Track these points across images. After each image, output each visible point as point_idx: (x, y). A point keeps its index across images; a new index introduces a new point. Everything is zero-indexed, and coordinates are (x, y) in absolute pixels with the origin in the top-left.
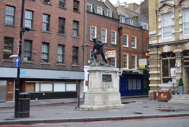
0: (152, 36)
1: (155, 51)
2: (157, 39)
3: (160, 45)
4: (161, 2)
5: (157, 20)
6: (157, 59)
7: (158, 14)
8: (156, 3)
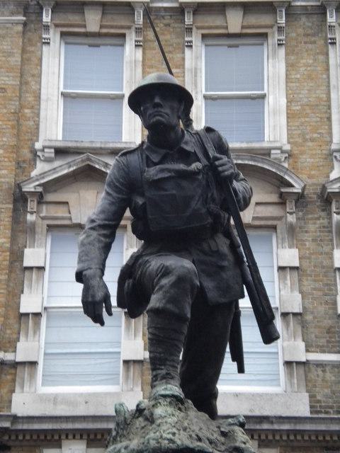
3: (24, 432)
4: (60, 152)
5: (17, 256)
7: (30, 218)
8: (16, 149)
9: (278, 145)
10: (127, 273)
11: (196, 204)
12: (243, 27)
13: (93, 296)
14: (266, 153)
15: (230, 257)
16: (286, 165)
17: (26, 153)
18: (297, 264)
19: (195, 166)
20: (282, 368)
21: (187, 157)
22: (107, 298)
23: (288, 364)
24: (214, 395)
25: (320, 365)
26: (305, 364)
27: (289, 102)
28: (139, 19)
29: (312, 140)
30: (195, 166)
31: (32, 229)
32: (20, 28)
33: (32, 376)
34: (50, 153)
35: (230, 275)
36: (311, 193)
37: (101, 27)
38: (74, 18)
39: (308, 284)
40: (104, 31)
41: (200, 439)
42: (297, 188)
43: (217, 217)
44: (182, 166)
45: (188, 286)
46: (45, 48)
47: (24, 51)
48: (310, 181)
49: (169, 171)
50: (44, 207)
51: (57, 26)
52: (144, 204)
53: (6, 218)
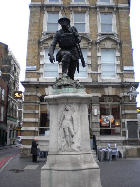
0: (29, 71)
1: (32, 92)
2: (37, 77)
3: (41, 85)
4: (47, 34)
5: (39, 54)
6: (36, 103)
8: (39, 33)
9: (88, 33)
10: (58, 54)
11: (71, 41)
12: (81, 10)
13: (51, 58)
14: (86, 34)
15: (77, 52)
16: (89, 37)
17: (40, 34)
18: (91, 55)
19: (71, 34)
20: (87, 74)
21: (69, 32)
22: (54, 59)
23: (88, 73)
24: (74, 77)
25: (94, 74)
26: (91, 73)
27: (90, 25)
28: (62, 9)
29: (94, 32)
30: (71, 34)
31: (41, 48)
32: (40, 11)
33: (43, 75)
34: (45, 34)
35: (77, 55)
36: (94, 42)
37: (55, 10)
38: (49, 9)
39: (93, 59)
40: (55, 11)
41: (70, 83)
42: (91, 41)
43: (75, 44)
44: (68, 34)
45: (69, 56)
46: (44, 15)
47: (40, 15)
48: (93, 40)
49: (66, 34)
50: (44, 44)
51: (46, 10)
52: (61, 41)
53: (37, 46)
